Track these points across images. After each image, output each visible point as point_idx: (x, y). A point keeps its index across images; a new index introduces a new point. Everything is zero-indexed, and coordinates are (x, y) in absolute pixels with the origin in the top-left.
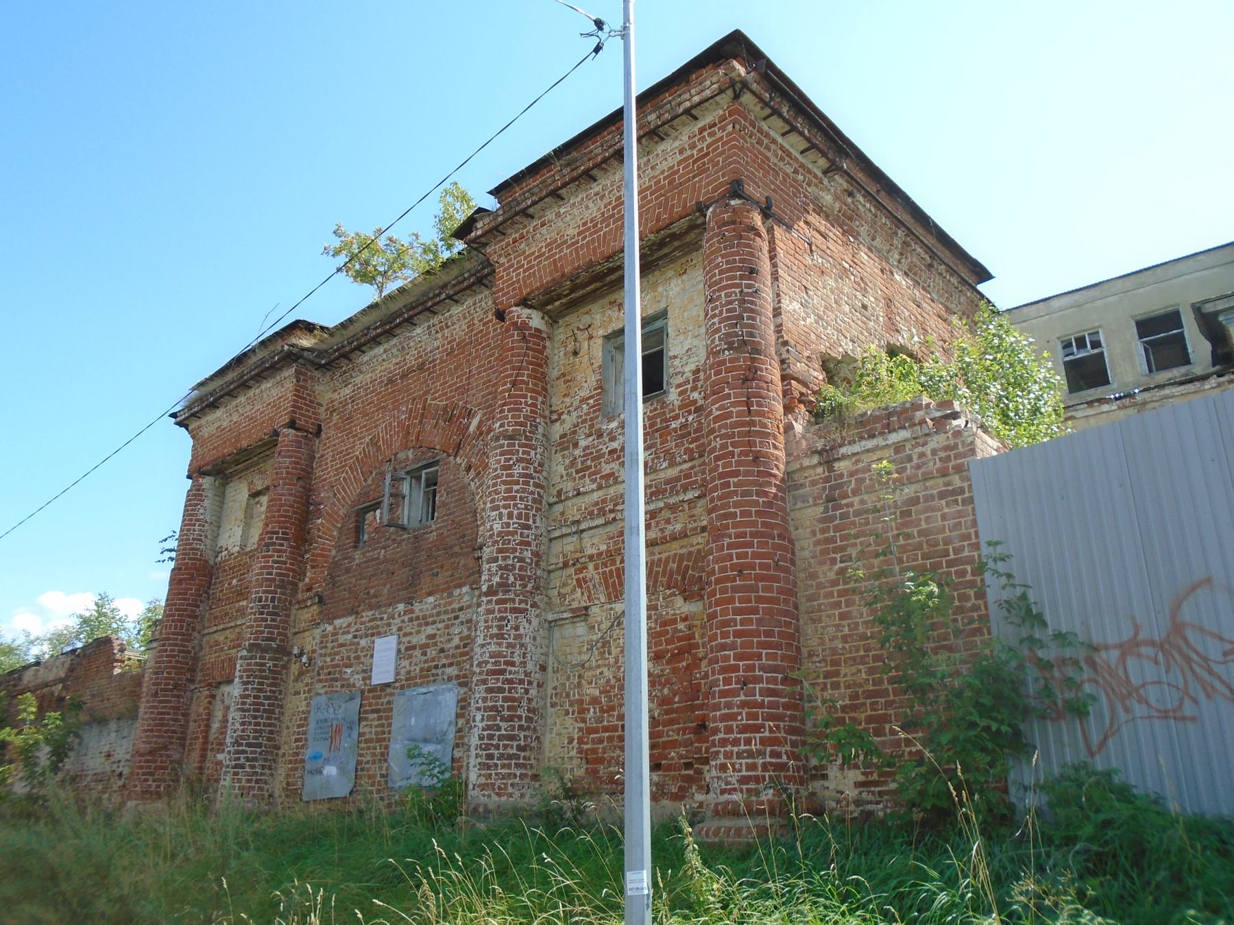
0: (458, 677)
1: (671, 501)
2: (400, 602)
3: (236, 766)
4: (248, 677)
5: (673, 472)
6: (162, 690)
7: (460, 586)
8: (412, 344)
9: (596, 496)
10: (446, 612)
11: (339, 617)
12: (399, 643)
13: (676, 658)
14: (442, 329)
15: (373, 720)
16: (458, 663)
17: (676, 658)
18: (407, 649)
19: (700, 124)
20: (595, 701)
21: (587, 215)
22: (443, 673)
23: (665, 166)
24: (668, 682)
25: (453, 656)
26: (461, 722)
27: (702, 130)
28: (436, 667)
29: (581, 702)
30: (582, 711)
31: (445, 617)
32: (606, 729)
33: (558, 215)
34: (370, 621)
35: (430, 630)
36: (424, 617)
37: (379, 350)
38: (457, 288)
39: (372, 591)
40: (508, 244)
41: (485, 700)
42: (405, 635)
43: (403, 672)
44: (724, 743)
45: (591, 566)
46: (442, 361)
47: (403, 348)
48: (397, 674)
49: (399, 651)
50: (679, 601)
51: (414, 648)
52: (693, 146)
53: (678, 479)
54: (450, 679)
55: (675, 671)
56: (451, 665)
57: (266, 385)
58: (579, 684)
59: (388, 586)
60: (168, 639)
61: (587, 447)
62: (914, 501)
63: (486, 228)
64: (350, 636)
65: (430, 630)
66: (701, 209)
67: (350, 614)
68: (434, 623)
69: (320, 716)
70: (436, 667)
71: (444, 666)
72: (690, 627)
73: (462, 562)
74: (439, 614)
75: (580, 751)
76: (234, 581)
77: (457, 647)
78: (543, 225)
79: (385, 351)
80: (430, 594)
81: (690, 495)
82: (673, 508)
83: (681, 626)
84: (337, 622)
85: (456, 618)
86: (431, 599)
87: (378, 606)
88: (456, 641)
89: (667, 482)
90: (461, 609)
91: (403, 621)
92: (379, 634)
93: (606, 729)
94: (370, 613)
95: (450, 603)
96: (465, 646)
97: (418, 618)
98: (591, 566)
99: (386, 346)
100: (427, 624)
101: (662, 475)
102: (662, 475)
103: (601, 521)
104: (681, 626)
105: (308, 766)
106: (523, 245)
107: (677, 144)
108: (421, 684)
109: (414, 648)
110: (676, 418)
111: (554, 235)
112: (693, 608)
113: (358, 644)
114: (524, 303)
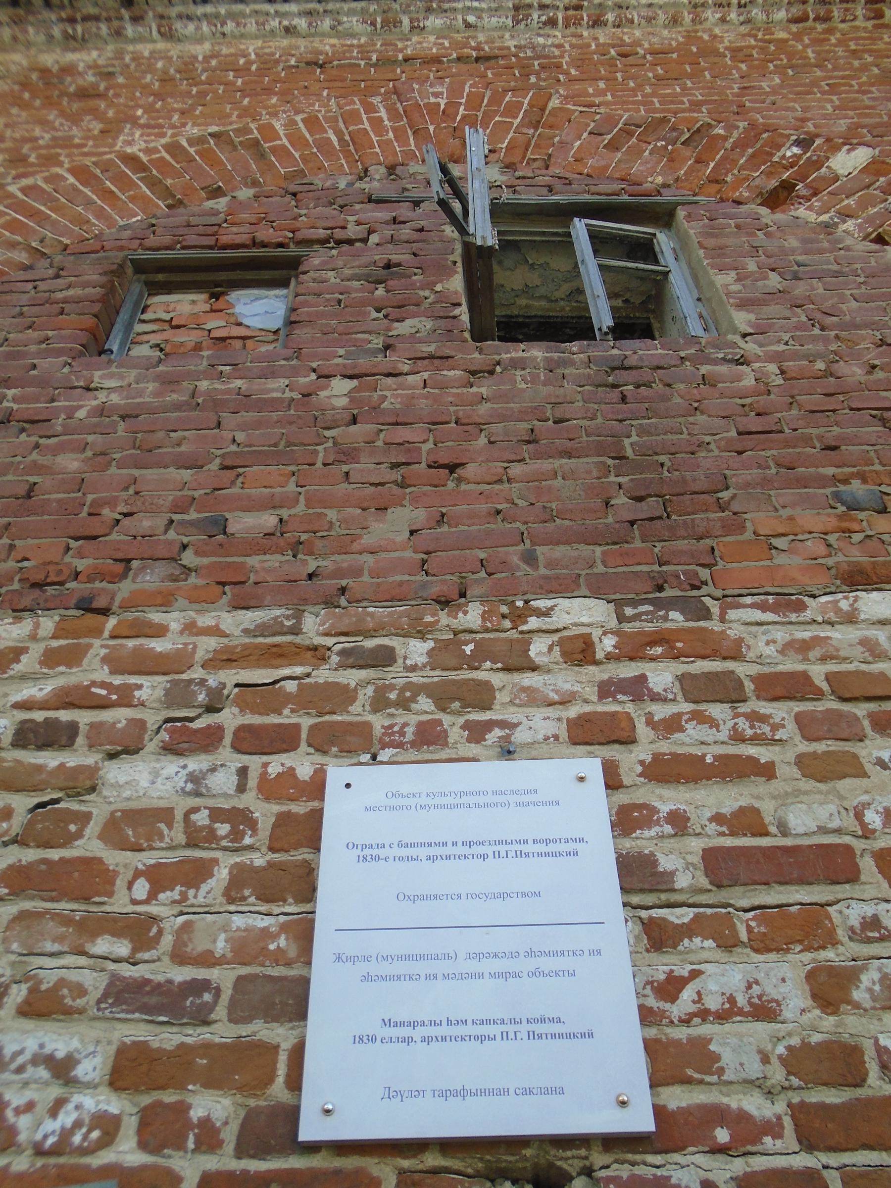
2: (565, 587)
12: (625, 821)
18: (720, 867)
34: (227, 659)
36: (845, 688)
39: (243, 523)
42: (662, 771)
43: (738, 1047)
48: (668, 1062)
91: (637, 688)
92: (356, 743)
94: (236, 623)
113: (84, 784)
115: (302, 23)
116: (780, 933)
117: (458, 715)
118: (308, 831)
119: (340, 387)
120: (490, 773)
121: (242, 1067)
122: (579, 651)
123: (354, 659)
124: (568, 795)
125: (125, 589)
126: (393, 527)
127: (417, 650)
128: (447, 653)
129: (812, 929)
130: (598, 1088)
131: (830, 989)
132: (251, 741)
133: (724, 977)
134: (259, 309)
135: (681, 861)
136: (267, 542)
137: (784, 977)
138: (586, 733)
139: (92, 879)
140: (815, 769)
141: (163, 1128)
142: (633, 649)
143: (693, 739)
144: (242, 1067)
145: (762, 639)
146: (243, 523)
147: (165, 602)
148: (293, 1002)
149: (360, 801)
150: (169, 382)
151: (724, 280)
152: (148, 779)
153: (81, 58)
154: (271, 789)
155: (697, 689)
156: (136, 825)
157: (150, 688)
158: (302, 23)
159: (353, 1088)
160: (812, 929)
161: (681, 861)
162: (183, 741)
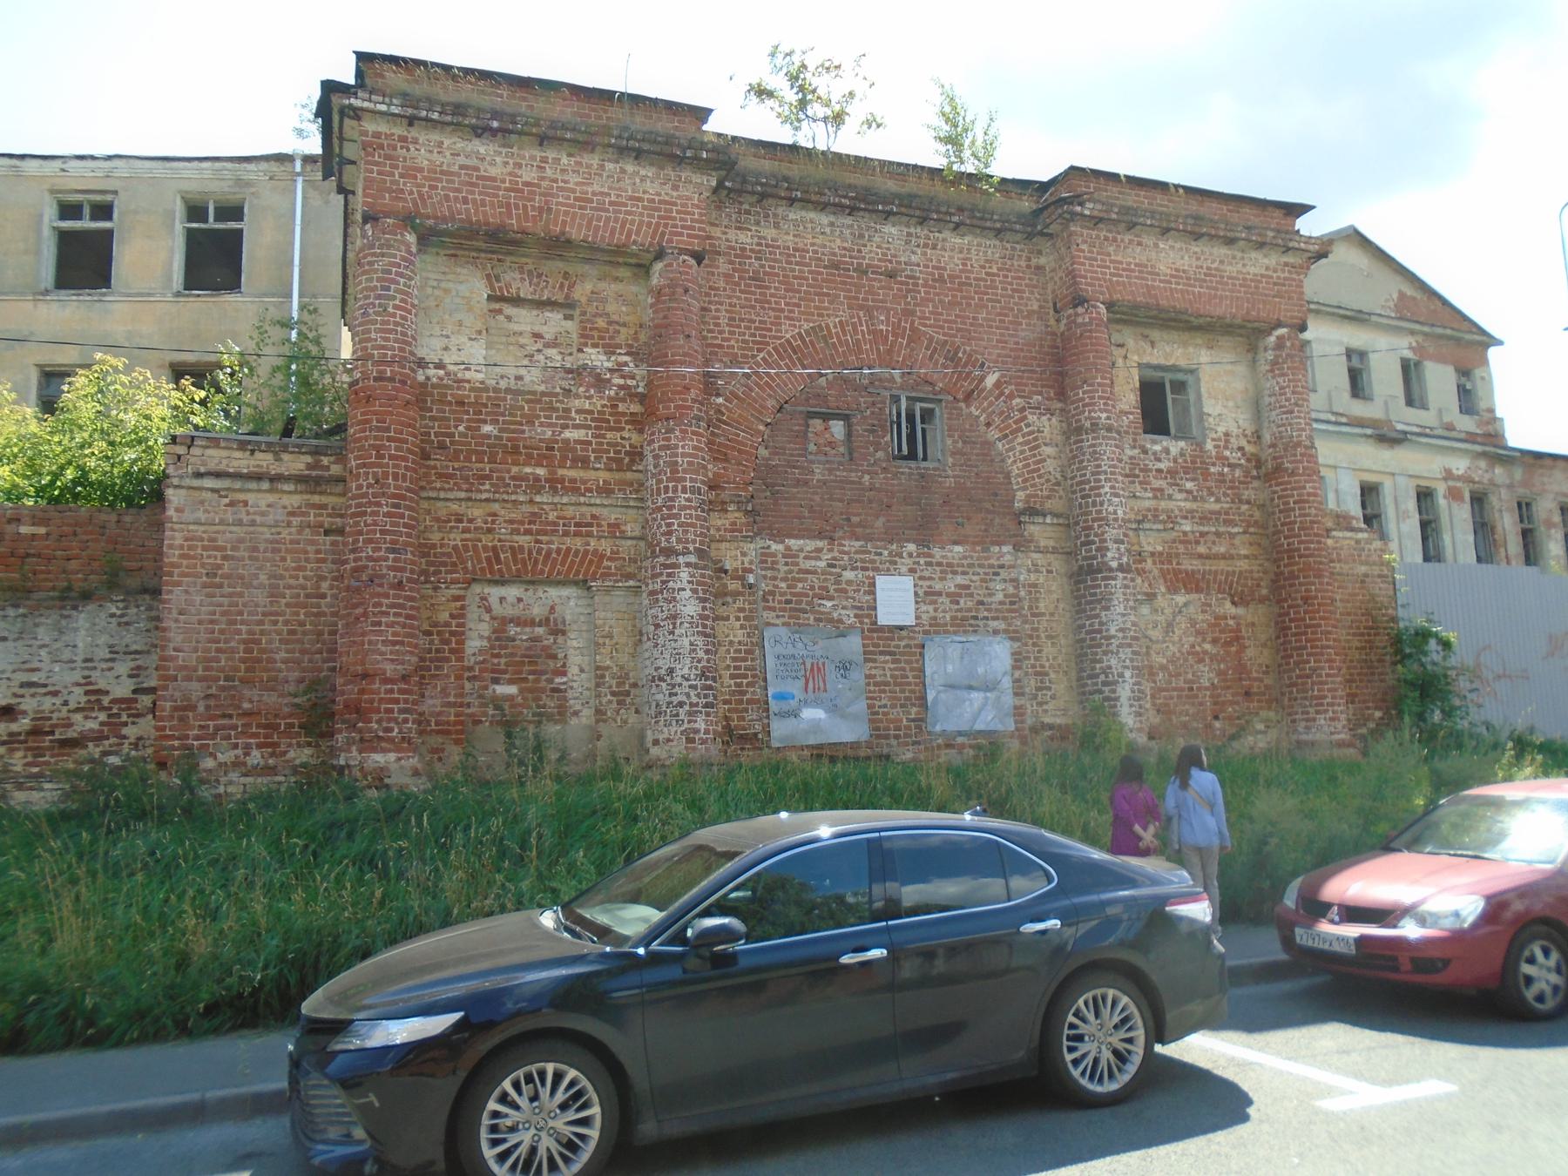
0: (1005, 631)
1: (1222, 529)
2: (908, 541)
3: (706, 705)
4: (705, 592)
5: (1217, 507)
6: (410, 580)
7: (1000, 544)
8: (876, 239)
9: (1147, 504)
10: (980, 566)
11: (791, 536)
13: (1228, 644)
14: (926, 246)
15: (886, 662)
16: (1004, 618)
17: (1228, 644)
18: (926, 593)
19: (1285, 259)
20: (1163, 668)
21: (1179, 264)
22: (986, 625)
23: (1252, 270)
24: (1223, 660)
25: (997, 610)
26: (1017, 674)
27: (1286, 264)
28: (976, 618)
29: (1151, 667)
30: (1152, 674)
31: (981, 571)
32: (1174, 689)
33: (1156, 245)
35: (960, 580)
36: (949, 565)
37: (825, 219)
38: (975, 222)
39: (855, 519)
40: (1098, 237)
41: (1132, 660)
42: (921, 578)
43: (924, 616)
44: (1332, 705)
45: (1149, 561)
46: (925, 285)
47: (861, 236)
48: (917, 618)
49: (916, 594)
50: (1228, 604)
51: (940, 594)
52: (1275, 271)
53: (1219, 513)
54: (996, 632)
55: (1228, 653)
56: (996, 618)
57: (648, 172)
58: (1148, 654)
59: (882, 520)
60: (403, 497)
61: (1131, 458)
62: (1366, 575)
63: (1096, 213)
64: (823, 564)
65: (960, 580)
66: (1279, 325)
67: (820, 535)
68: (964, 573)
69: (779, 649)
70: (976, 618)
71: (986, 618)
72: (1238, 624)
73: (997, 521)
74: (970, 566)
75: (1154, 704)
76: (487, 429)
77: (1001, 603)
78: (1139, 244)
79: (832, 224)
80: (956, 543)
81: (1236, 530)
82: (1218, 534)
83: (1231, 622)
84: (792, 542)
85: (997, 574)
86: (958, 549)
87: (868, 538)
88: (1000, 596)
89: (1212, 512)
90: (1002, 566)
93: (1174, 689)
94: (858, 544)
95: (987, 558)
96: (1012, 603)
97: (939, 564)
98: (1149, 561)
99: (832, 218)
100: (954, 573)
101: (1207, 506)
102: (1207, 506)
103: (1160, 527)
104: (1231, 622)
105: (774, 706)
106: (1111, 249)
107: (1266, 261)
108: (955, 633)
109: (940, 594)
110: (1214, 464)
111: (1144, 259)
112: (1240, 611)
114: (1110, 306)
115: (828, 230)
116: (931, 603)
117: (891, 569)
118: (874, 585)
119: (867, 477)
120: (898, 578)
121: (869, 616)
122: (910, 555)
123: (877, 554)
124: (908, 582)
125: (837, 535)
126: (880, 523)
127: (886, 553)
128: (890, 554)
129: (935, 602)
130: (909, 620)
131: (936, 610)
132: (863, 569)
133: (924, 608)
134: (837, 428)
135: (921, 592)
136: (859, 525)
137: (931, 608)
138: (912, 571)
139: (845, 591)
140: (942, 579)
141: (861, 623)
142: (919, 556)
143: (926, 574)
144: (869, 616)
145: (937, 553)
146: (855, 519)
147: (843, 538)
148: (875, 608)
149: (881, 581)
150: (830, 470)
151: (949, 442)
152: (849, 575)
153: (745, 238)
154: (868, 577)
155: (929, 564)
156: (849, 582)
157: (846, 557)
158: (828, 230)
159: (884, 619)
160: (935, 602)
161: (921, 592)
162: (855, 569)
